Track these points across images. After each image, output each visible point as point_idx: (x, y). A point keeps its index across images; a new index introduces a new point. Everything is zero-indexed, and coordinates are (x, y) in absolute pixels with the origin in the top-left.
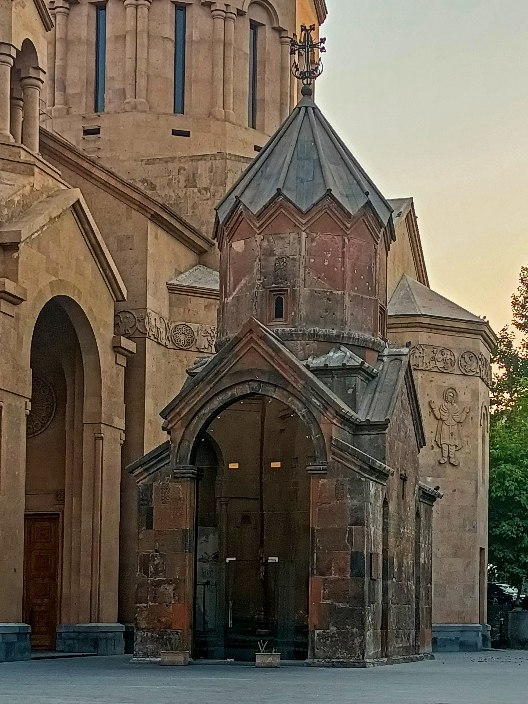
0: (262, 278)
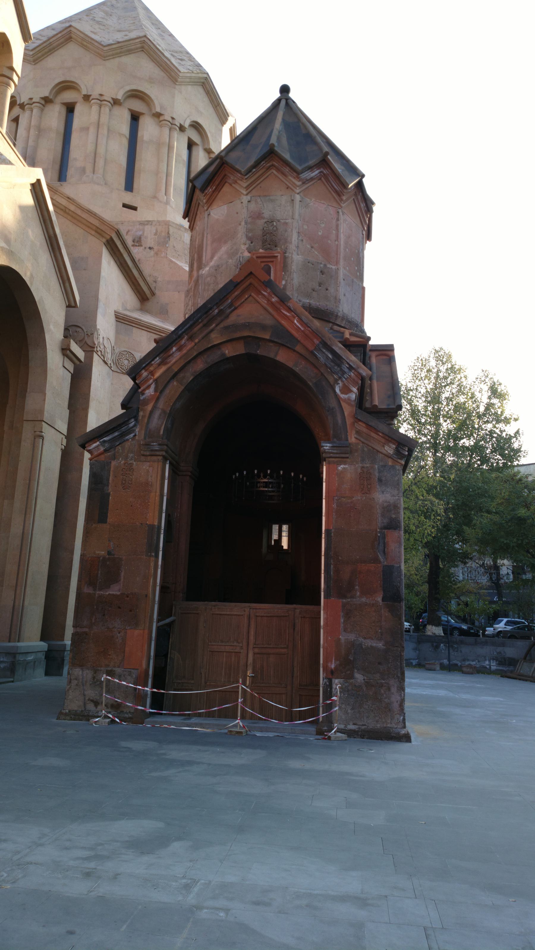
0: (248, 242)
